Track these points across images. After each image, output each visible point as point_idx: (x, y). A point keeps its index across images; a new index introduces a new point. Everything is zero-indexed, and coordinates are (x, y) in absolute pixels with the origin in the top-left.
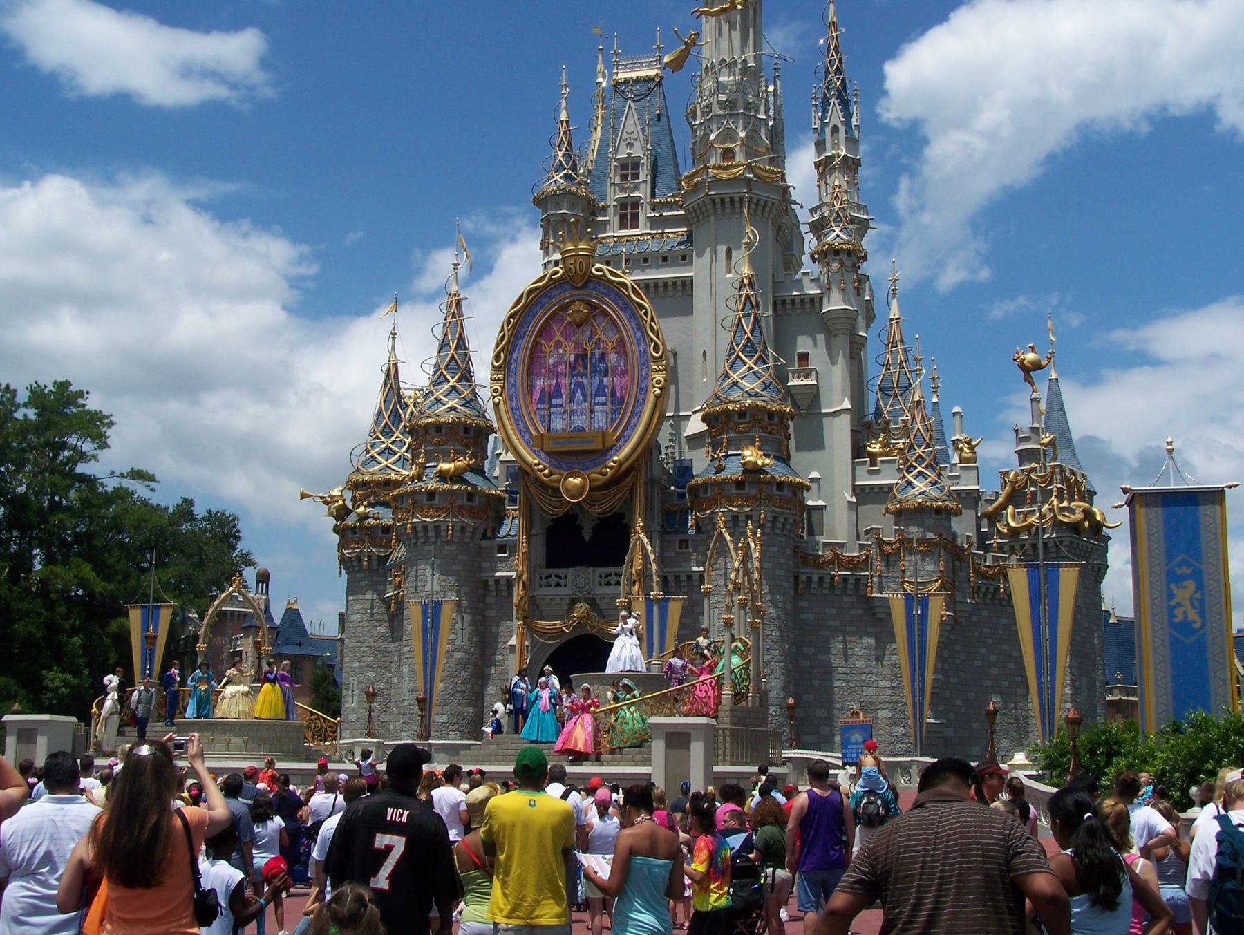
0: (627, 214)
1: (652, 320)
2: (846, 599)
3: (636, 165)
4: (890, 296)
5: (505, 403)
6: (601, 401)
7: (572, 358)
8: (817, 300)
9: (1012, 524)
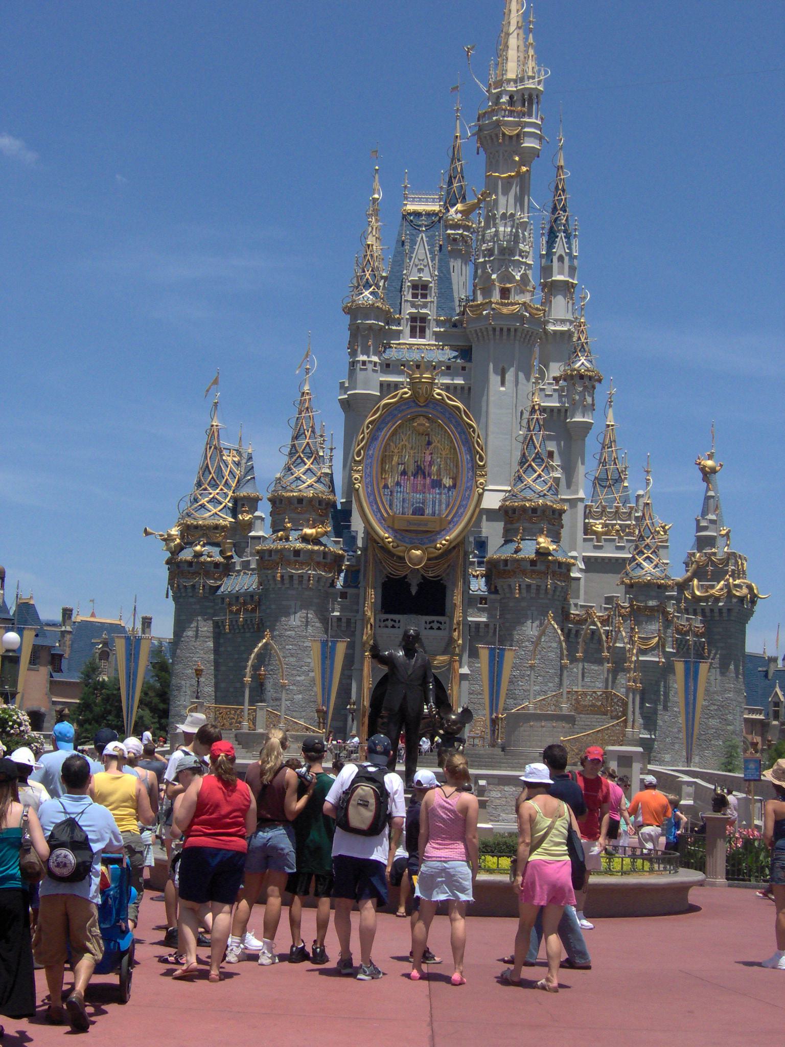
0: (416, 327)
1: (478, 437)
4: (608, 406)
9: (698, 593)
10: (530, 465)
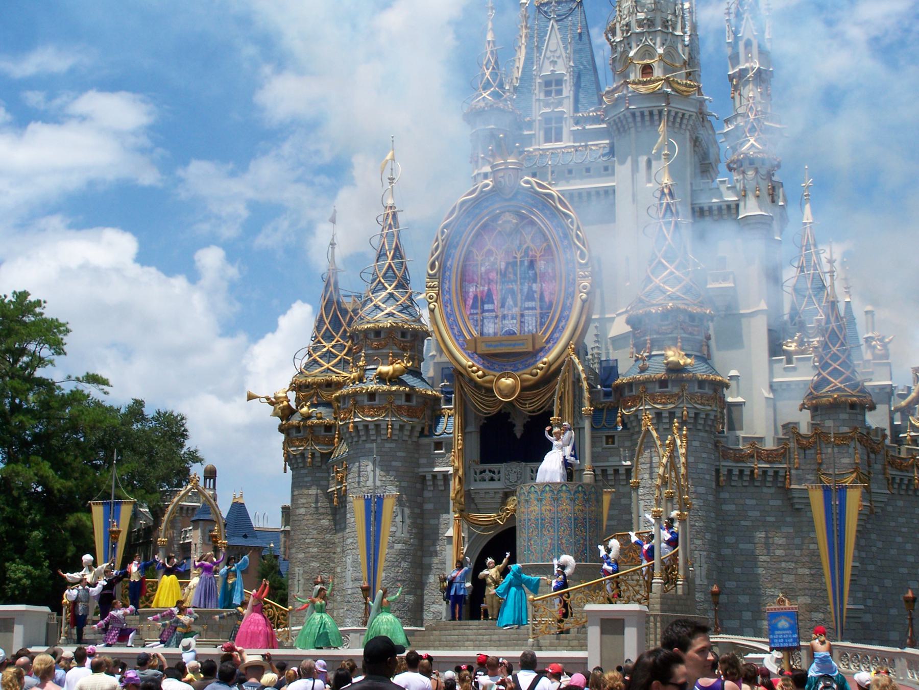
0: (550, 129)
1: (578, 228)
2: (765, 490)
3: (559, 82)
5: (440, 308)
6: (530, 306)
7: (503, 265)
8: (733, 206)
10: (660, 262)
